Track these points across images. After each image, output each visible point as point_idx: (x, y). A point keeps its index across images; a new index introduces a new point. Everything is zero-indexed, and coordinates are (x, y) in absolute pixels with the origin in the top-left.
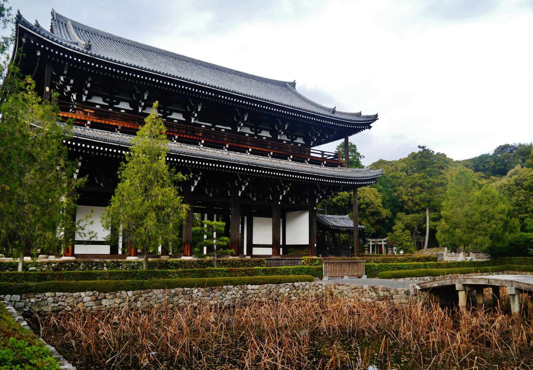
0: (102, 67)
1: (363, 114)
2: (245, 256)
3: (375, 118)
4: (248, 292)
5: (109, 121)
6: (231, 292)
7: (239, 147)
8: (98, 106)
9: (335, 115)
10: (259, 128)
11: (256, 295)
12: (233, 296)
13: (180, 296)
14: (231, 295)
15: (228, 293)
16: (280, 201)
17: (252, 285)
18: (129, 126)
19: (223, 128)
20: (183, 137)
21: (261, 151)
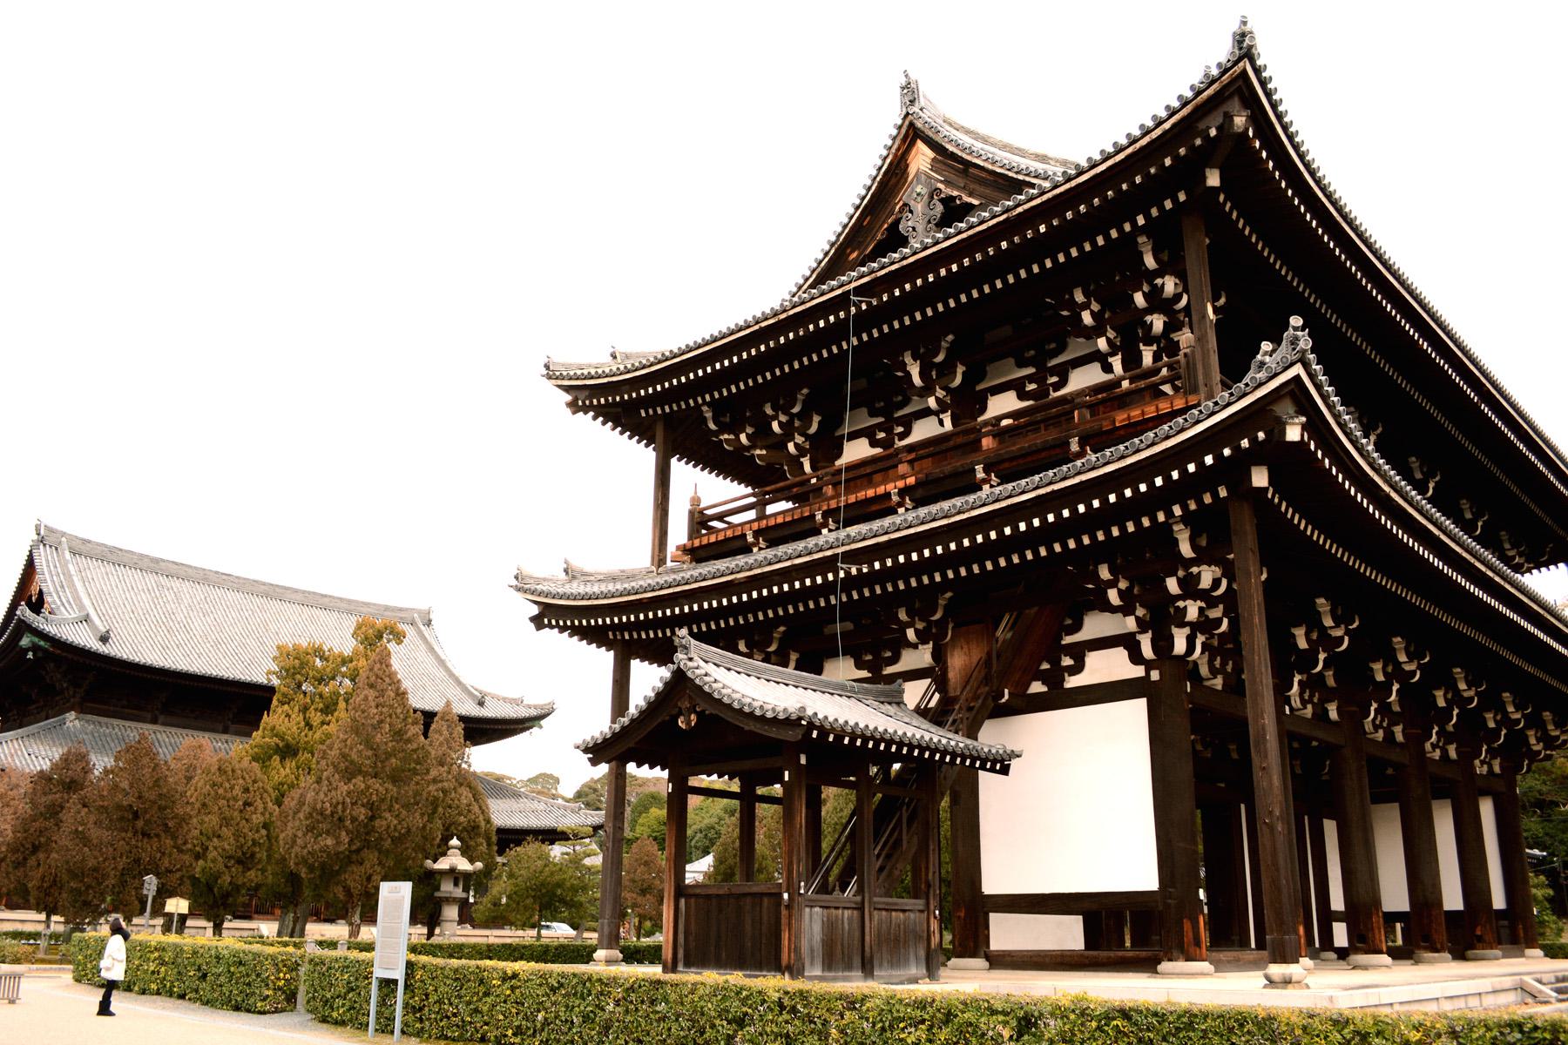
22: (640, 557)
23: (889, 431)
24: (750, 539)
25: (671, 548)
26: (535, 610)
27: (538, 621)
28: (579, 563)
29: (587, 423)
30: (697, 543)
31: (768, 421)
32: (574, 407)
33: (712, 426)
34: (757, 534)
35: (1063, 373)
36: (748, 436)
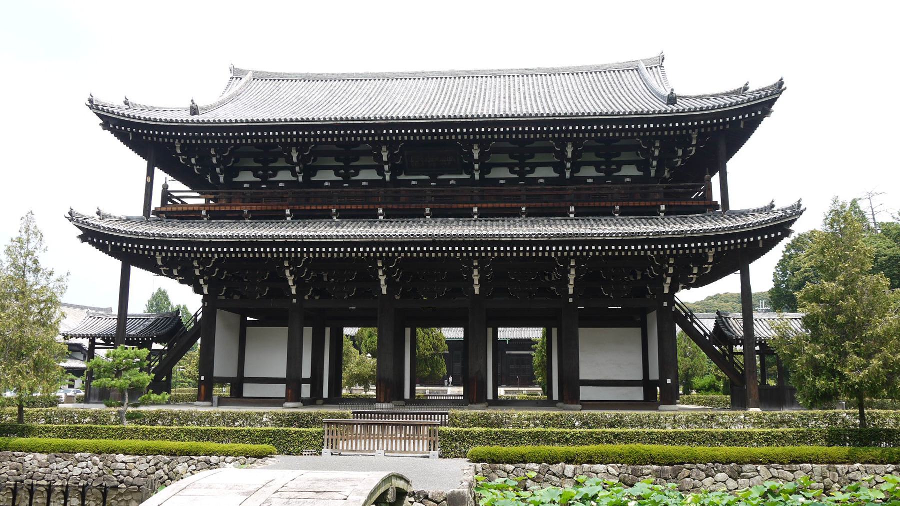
1: (752, 88)
3: (779, 88)
6: (84, 464)
7: (451, 209)
8: (246, 185)
9: (681, 105)
10: (529, 164)
11: (125, 472)
12: (88, 470)
13: (5, 463)
15: (80, 465)
16: (571, 296)
17: (125, 454)
18: (259, 208)
21: (500, 208)
22: (139, 212)
23: (265, 171)
24: (204, 213)
25: (153, 209)
26: (81, 233)
28: (104, 211)
29: (108, 136)
30: (164, 209)
32: (105, 126)
33: (179, 151)
34: (207, 212)
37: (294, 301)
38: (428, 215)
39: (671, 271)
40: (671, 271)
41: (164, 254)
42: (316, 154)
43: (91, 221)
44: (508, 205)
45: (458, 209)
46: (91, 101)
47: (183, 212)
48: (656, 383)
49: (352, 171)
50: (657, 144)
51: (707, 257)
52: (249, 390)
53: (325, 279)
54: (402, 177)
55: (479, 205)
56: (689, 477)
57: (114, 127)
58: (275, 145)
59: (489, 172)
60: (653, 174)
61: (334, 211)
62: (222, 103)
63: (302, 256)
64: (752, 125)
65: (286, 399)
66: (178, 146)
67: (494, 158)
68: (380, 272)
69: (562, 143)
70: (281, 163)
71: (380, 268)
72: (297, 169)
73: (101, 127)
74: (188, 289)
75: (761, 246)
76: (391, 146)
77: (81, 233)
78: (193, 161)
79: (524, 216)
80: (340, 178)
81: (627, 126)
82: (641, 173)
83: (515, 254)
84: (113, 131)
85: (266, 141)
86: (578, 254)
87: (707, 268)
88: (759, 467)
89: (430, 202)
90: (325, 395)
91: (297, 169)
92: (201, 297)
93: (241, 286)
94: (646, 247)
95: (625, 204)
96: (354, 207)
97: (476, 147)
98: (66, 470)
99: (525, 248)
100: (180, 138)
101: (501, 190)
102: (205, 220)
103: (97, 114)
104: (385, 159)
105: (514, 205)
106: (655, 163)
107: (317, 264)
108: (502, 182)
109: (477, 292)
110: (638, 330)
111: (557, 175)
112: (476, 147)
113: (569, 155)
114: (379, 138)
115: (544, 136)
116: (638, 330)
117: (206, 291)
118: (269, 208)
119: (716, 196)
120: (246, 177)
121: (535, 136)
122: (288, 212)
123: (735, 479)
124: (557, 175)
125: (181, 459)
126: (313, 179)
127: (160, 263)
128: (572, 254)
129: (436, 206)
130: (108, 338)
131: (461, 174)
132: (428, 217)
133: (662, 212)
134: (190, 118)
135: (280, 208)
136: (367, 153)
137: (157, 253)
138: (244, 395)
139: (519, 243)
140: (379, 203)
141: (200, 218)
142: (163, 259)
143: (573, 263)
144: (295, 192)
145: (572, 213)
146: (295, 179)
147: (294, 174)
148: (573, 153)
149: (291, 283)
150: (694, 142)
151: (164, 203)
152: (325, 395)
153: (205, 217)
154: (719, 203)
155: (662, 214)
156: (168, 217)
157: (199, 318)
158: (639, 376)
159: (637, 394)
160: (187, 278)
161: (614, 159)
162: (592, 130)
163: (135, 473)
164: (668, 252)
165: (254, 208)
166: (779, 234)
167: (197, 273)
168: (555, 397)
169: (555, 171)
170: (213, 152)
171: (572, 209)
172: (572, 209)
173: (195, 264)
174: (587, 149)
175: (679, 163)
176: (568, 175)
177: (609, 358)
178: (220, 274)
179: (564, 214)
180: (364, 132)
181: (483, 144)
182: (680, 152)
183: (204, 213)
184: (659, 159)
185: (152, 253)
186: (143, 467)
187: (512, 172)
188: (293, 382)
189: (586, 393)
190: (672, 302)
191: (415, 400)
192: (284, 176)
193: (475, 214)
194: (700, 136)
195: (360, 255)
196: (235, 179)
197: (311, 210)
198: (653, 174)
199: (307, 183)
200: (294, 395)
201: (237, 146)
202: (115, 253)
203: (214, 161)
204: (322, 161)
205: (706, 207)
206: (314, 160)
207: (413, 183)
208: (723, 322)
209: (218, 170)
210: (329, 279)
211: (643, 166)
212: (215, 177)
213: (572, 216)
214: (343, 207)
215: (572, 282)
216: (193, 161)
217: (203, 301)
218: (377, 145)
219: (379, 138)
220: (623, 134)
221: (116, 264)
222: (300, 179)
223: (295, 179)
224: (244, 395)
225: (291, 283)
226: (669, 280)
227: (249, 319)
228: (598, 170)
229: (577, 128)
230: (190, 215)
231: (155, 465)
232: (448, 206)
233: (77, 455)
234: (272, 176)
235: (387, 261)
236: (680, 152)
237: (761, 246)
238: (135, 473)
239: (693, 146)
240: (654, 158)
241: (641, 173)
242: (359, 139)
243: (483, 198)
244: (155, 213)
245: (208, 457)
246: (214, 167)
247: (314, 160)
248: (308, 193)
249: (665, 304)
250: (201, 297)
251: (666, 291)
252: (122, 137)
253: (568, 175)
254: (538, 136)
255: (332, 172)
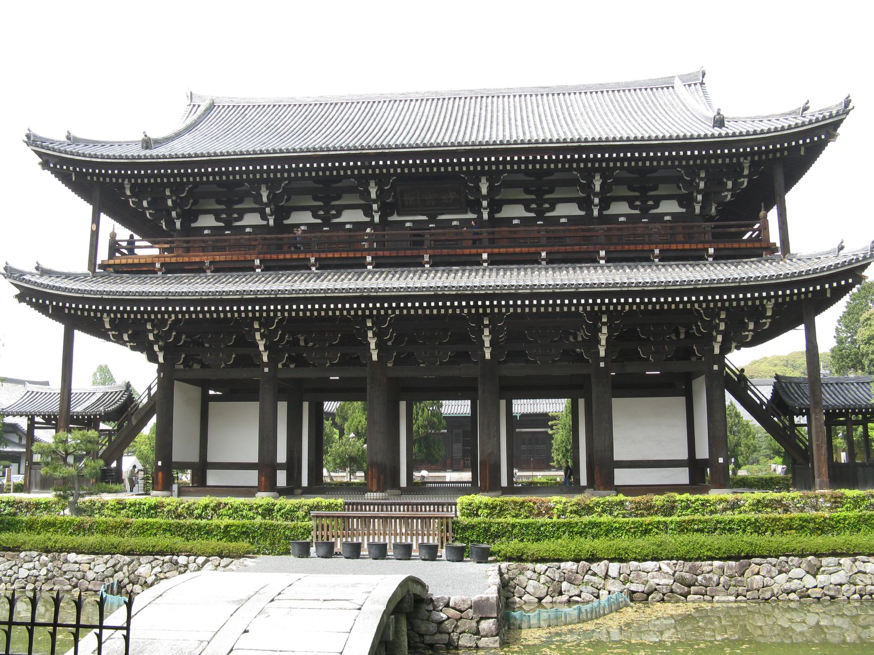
0: (149, 171)
2: (584, 488)
4: (65, 567)
5: (189, 257)
6: (31, 565)
8: (206, 232)
9: (731, 128)
11: (79, 575)
12: (35, 572)
14: (29, 570)
16: (603, 359)
17: (78, 553)
18: (223, 258)
19: (455, 218)
20: (327, 258)
21: (514, 254)
22: (82, 266)
23: (229, 215)
24: (158, 266)
25: (99, 262)
26: (18, 292)
27: (21, 298)
28: (46, 265)
29: (48, 177)
30: (112, 262)
31: (165, 198)
32: (45, 165)
33: (128, 193)
34: (162, 265)
35: (340, 210)
36: (148, 203)
37: (266, 370)
38: (427, 263)
39: (722, 327)
40: (722, 327)
41: (112, 316)
42: (290, 192)
43: (27, 277)
44: (525, 250)
45: (463, 255)
46: (28, 136)
47: (133, 265)
48: (704, 463)
49: (334, 212)
50: (703, 175)
51: (765, 309)
52: (213, 478)
53: (302, 343)
54: (395, 218)
55: (490, 250)
56: (758, 574)
57: (55, 166)
58: (241, 183)
59: (499, 211)
60: (697, 210)
61: (313, 260)
62: (178, 135)
63: (276, 316)
64: (814, 151)
65: (259, 488)
66: (128, 187)
67: (505, 194)
68: (370, 334)
69: (589, 174)
70: (248, 204)
71: (370, 328)
72: (268, 210)
73: (40, 167)
74: (141, 357)
75: (828, 295)
76: (381, 180)
77: (18, 292)
78: (145, 204)
79: (544, 263)
80: (319, 221)
81: (667, 154)
82: (684, 210)
83: (534, 310)
84: (54, 171)
85: (231, 178)
86: (612, 308)
87: (765, 323)
88: (843, 560)
89: (430, 248)
90: (305, 483)
91: (268, 210)
92: (156, 366)
93: (204, 353)
94: (694, 298)
95: (666, 247)
96: (337, 255)
97: (484, 180)
98: (10, 572)
99: (547, 302)
100: (130, 177)
101: (515, 232)
102: (160, 273)
103: (36, 152)
104: (373, 196)
105: (532, 250)
106: (700, 198)
107: (293, 324)
108: (515, 222)
109: (488, 356)
110: (683, 399)
111: (583, 213)
112: (484, 180)
113: (598, 188)
114: (367, 171)
115: (567, 166)
116: (683, 399)
117: (161, 360)
118: (235, 258)
119: (774, 237)
120: (207, 221)
121: (556, 166)
122: (257, 262)
123: (814, 576)
124: (583, 213)
125: (144, 559)
126: (286, 222)
127: (107, 326)
128: (604, 308)
129: (437, 252)
130: (49, 416)
131: (466, 213)
132: (427, 266)
133: (710, 256)
134: (143, 153)
135: (248, 257)
136: (352, 190)
137: (105, 315)
138: (208, 484)
139: (539, 296)
140: (366, 250)
141: (155, 272)
142: (112, 321)
143: (604, 320)
144: (265, 239)
145: (602, 258)
146: (265, 223)
147: (264, 217)
148: (602, 186)
149: (262, 348)
150: (746, 172)
151: (111, 255)
152: (305, 483)
153: (160, 270)
154: (778, 245)
155: (711, 259)
156: (116, 272)
157: (153, 392)
158: (684, 455)
159: (682, 476)
160: (140, 343)
161: (651, 193)
162: (625, 158)
163: (90, 575)
164: (719, 304)
165: (217, 258)
166: (850, 281)
167: (151, 337)
168: (584, 481)
169: (580, 208)
170: (168, 193)
171: (602, 253)
172: (602, 253)
173: (149, 327)
174: (618, 181)
175: (729, 197)
176: (596, 213)
177: (649, 434)
178: (178, 338)
179: (592, 260)
180: (348, 164)
181: (492, 177)
182: (730, 184)
183: (158, 266)
184: (706, 194)
185: (99, 315)
186: (100, 568)
187: (528, 209)
188: (266, 466)
189: (622, 477)
190: (723, 365)
191: (415, 488)
192: (252, 220)
193: (485, 261)
194: (753, 164)
195: (345, 313)
196: (193, 225)
197: (285, 260)
198: (697, 210)
199: (280, 227)
200: (268, 484)
201: (196, 185)
202: (57, 314)
203: (170, 203)
204: (296, 201)
205: (761, 249)
206: (288, 200)
207: (408, 224)
208: (783, 388)
209: (174, 214)
210: (306, 342)
211: (686, 201)
212: (171, 223)
213: (602, 262)
214: (323, 255)
215: (603, 342)
216: (145, 204)
217: (159, 371)
218: (364, 180)
219: (367, 171)
220: (662, 163)
221: (58, 328)
222: (271, 222)
223: (265, 223)
224: (208, 484)
225: (262, 348)
226: (720, 338)
227: (211, 392)
228: (632, 207)
229: (607, 155)
230: (143, 269)
231: (113, 566)
232: (451, 252)
233: (23, 554)
234: (237, 220)
235: (378, 320)
236: (730, 184)
237: (828, 295)
238: (90, 575)
239: (745, 177)
240: (699, 192)
241: (684, 210)
242: (342, 173)
243: (493, 242)
244: (101, 267)
245: (175, 557)
246: (169, 211)
247: (288, 200)
248: (282, 239)
249: (716, 367)
250: (156, 366)
251: (717, 351)
252: (64, 177)
253: (596, 213)
254: (560, 166)
255: (309, 214)
